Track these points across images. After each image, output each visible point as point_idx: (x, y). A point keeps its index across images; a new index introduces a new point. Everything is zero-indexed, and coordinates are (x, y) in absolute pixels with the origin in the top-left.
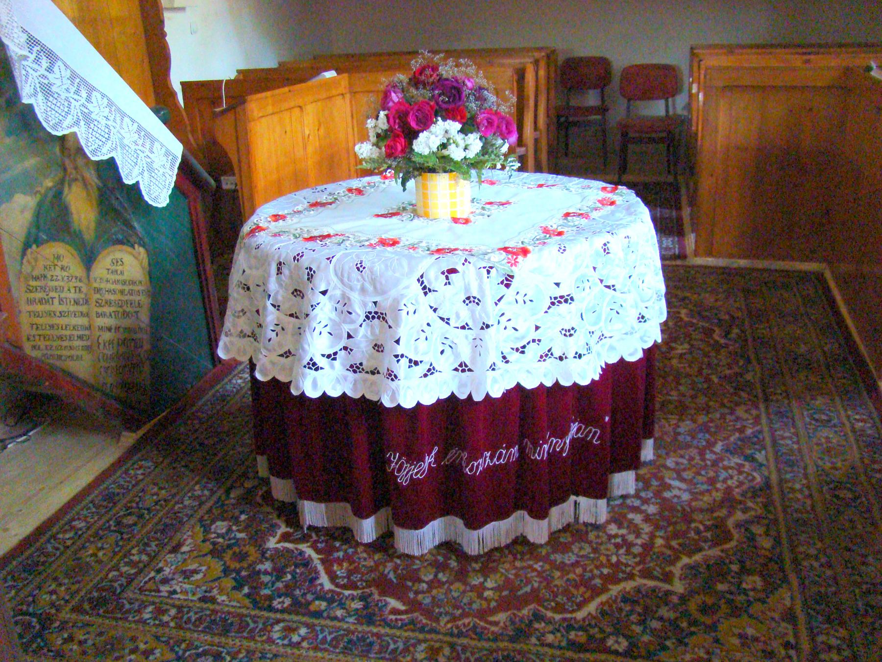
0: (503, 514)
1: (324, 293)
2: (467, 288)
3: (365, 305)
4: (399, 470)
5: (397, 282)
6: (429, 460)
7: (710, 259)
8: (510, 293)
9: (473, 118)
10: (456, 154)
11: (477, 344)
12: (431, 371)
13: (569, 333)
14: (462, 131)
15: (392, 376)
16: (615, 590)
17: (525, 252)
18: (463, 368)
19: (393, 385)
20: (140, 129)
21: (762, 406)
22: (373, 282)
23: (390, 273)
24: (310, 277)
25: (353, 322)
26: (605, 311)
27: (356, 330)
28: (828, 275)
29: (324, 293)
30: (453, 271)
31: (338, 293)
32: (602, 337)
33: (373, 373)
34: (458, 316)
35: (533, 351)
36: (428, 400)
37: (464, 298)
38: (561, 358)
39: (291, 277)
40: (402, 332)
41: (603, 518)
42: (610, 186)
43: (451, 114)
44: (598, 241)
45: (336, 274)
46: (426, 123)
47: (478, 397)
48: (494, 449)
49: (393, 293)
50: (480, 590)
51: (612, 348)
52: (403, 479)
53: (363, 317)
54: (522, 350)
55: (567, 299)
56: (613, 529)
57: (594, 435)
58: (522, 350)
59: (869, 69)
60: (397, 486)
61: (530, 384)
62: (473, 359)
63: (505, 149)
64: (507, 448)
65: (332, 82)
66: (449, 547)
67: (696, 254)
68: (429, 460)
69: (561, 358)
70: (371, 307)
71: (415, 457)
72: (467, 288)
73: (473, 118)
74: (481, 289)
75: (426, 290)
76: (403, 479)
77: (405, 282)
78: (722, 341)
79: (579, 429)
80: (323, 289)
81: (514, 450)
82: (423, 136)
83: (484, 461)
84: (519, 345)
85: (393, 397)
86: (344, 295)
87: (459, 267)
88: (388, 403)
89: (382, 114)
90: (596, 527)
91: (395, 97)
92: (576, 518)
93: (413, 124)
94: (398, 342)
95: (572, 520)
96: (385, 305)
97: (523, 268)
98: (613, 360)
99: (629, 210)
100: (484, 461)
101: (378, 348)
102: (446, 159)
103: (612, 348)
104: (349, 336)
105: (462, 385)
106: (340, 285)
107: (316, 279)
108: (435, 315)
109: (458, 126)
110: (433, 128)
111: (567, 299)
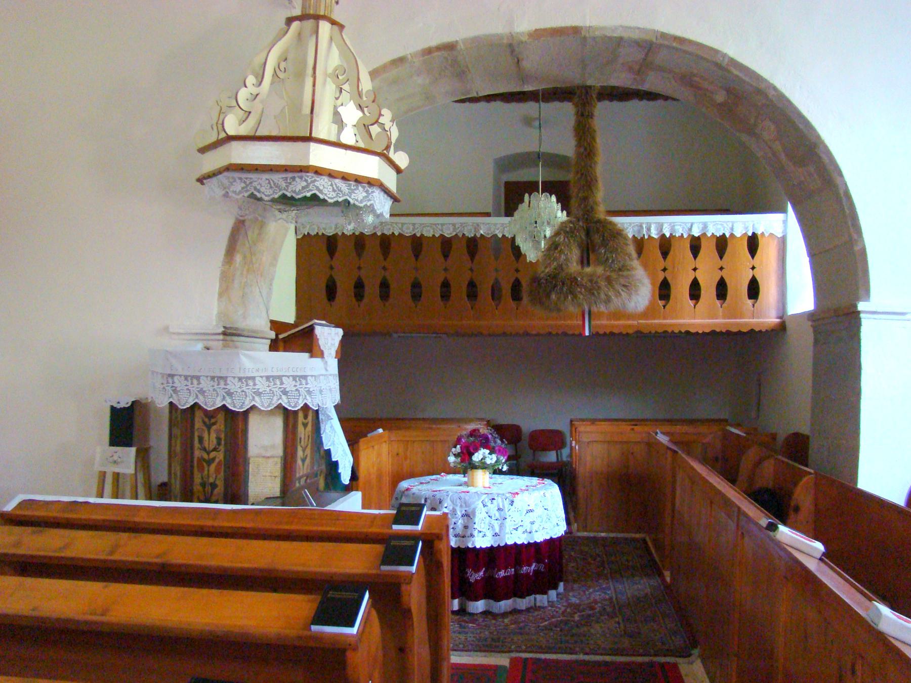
0: (507, 598)
1: (446, 507)
2: (498, 505)
3: (461, 511)
4: (471, 576)
5: (474, 503)
6: (481, 573)
7: (585, 533)
8: (512, 508)
9: (494, 448)
10: (488, 461)
11: (502, 526)
12: (484, 536)
13: (532, 523)
14: (489, 454)
15: (472, 535)
16: (553, 620)
17: (517, 494)
18: (496, 535)
19: (473, 539)
20: (344, 450)
21: (610, 580)
22: (465, 503)
23: (471, 500)
24: (440, 502)
25: (457, 518)
26: (545, 518)
27: (458, 521)
28: (648, 539)
29: (446, 507)
30: (493, 499)
31: (451, 508)
32: (543, 528)
33: (463, 537)
34: (495, 515)
35: (521, 530)
36: (484, 546)
37: (497, 508)
38: (530, 533)
39: (431, 504)
40: (477, 520)
41: (546, 604)
42: (541, 479)
43: (486, 446)
44: (542, 493)
45: (451, 500)
46: (477, 450)
47: (502, 544)
48: (506, 569)
49: (473, 506)
50: (503, 622)
51: (547, 533)
52: (472, 580)
53: (460, 516)
54: (516, 529)
55: (531, 511)
56: (550, 608)
57: (542, 567)
58: (516, 529)
59: (656, 433)
60: (470, 582)
61: (519, 542)
62: (500, 530)
63: (504, 461)
64: (511, 569)
65: (380, 436)
66: (486, 613)
67: (578, 530)
68: (481, 573)
69: (530, 533)
70: (464, 512)
71: (477, 570)
72: (498, 505)
73: (494, 448)
74: (503, 506)
75: (484, 506)
76: (472, 580)
77: (477, 503)
78: (592, 562)
79: (535, 566)
80: (445, 506)
81: (513, 570)
82: (476, 454)
83: (502, 573)
84: (516, 527)
85: (473, 543)
86: (453, 508)
87: (496, 498)
88: (470, 546)
89: (458, 446)
90: (544, 608)
91: (463, 440)
92: (535, 604)
93: (472, 451)
94: (475, 523)
95: (534, 606)
96: (470, 510)
97: (517, 499)
98: (548, 538)
99: (550, 485)
100: (502, 573)
101: (466, 527)
102: (485, 463)
103: (547, 533)
104: (455, 523)
105: (495, 542)
106: (452, 505)
107: (443, 503)
108: (487, 515)
109: (487, 451)
110: (480, 452)
111: (531, 511)
